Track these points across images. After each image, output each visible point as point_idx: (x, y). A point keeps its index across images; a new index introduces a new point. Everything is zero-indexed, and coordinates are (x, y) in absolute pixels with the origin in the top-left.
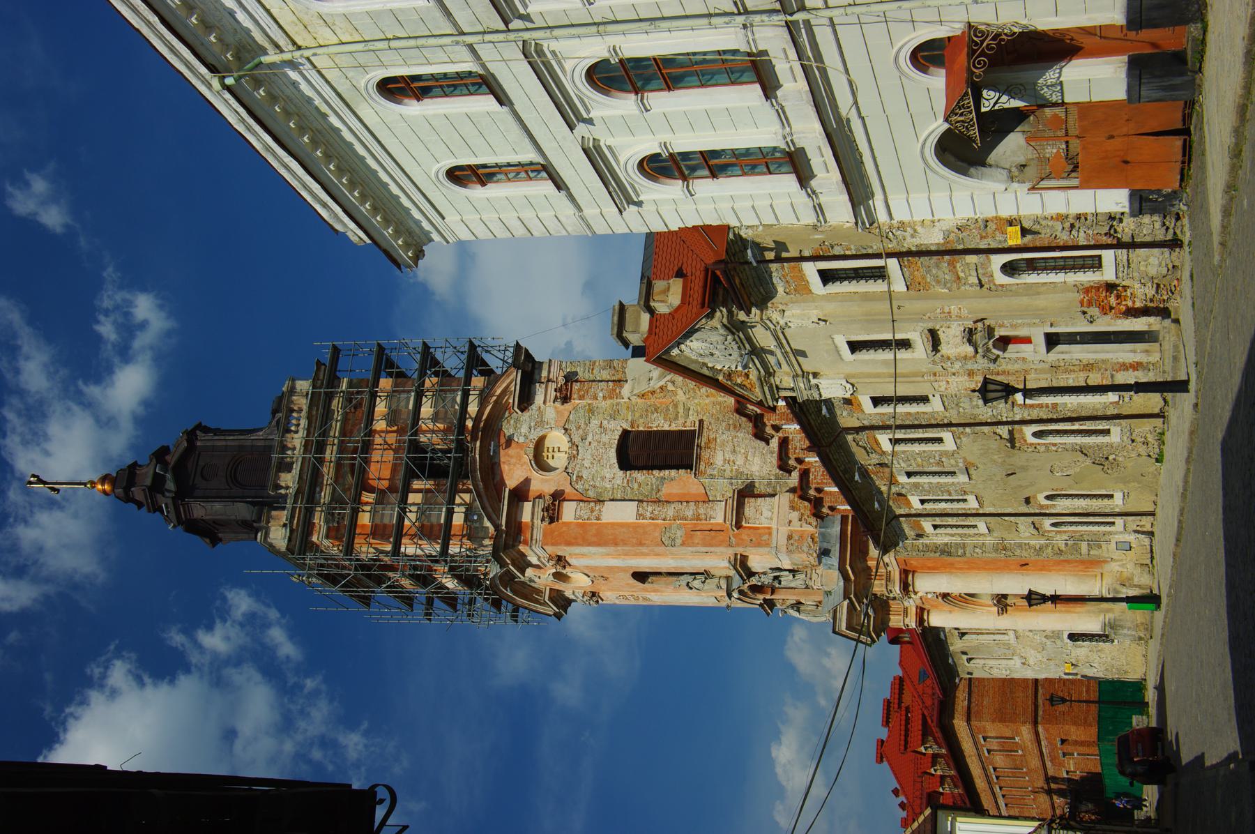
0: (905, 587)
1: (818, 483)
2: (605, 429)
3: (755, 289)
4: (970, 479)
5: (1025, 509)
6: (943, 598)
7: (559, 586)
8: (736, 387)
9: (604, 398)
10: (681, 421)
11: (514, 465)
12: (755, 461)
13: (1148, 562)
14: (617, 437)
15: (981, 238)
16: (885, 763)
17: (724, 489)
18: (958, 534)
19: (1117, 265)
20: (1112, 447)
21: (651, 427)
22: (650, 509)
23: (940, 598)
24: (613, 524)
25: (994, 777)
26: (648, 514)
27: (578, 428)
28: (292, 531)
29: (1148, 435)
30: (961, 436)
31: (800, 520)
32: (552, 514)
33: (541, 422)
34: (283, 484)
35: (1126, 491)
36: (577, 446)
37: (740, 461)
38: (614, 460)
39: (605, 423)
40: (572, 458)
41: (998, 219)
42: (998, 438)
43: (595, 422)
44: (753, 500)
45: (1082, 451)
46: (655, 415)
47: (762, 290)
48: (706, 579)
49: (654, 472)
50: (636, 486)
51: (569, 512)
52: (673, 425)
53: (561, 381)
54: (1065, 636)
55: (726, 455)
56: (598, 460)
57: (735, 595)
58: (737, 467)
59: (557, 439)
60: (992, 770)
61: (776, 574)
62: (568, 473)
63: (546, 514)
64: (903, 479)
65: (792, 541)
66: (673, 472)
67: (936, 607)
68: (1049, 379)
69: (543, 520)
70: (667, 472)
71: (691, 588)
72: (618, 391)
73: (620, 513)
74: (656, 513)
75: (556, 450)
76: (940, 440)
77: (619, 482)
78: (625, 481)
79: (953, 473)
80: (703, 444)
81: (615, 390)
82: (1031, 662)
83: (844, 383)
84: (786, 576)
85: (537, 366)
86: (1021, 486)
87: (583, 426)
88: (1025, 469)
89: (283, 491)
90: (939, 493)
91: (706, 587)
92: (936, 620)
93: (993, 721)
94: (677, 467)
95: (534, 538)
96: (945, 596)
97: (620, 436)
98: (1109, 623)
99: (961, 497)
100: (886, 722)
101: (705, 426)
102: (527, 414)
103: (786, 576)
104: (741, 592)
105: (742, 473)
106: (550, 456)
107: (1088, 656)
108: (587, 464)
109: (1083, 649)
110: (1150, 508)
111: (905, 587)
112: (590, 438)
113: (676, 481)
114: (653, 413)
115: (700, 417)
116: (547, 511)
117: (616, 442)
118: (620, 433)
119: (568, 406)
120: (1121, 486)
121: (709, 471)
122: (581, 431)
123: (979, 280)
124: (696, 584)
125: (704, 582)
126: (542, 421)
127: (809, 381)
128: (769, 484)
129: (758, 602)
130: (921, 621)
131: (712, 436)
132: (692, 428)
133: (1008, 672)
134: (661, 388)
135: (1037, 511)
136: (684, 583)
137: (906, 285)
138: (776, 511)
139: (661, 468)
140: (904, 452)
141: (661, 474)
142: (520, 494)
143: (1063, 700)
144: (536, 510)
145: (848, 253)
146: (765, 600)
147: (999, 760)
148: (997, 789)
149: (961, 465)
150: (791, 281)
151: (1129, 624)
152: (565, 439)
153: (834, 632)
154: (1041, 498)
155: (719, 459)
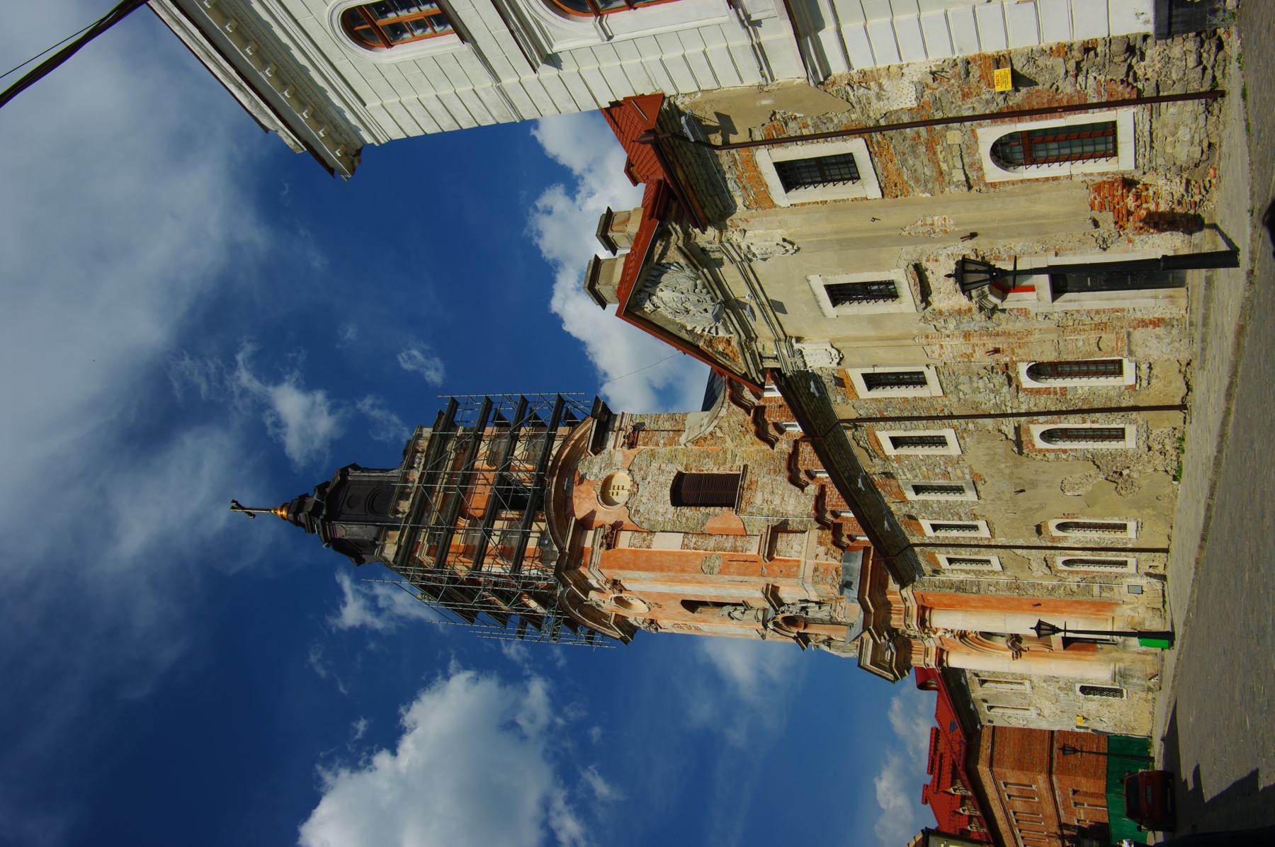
0: (922, 622)
1: (833, 506)
2: (663, 471)
3: (709, 199)
4: (979, 497)
5: (1035, 541)
6: (960, 639)
7: (623, 612)
8: (718, 356)
9: (665, 445)
10: (728, 465)
11: (584, 499)
12: (790, 502)
13: (1160, 606)
14: (672, 478)
15: (964, 95)
16: (929, 805)
17: (759, 525)
18: (973, 571)
19: (1136, 140)
20: (1127, 457)
21: (702, 471)
22: (694, 540)
23: (957, 638)
24: (661, 553)
25: (1014, 820)
27: (641, 469)
28: (399, 547)
29: (1167, 441)
30: (965, 435)
31: (826, 554)
32: (610, 541)
33: (610, 464)
34: (401, 510)
35: (1140, 520)
36: (638, 485)
37: (777, 501)
38: (668, 497)
39: (663, 466)
40: (632, 494)
41: (984, 58)
42: (1004, 437)
43: (655, 465)
45: (1094, 460)
46: (707, 460)
47: (718, 202)
48: (745, 610)
49: (701, 509)
50: (684, 520)
51: (624, 540)
52: (721, 469)
53: (630, 430)
54: (1078, 689)
57: (770, 625)
58: (773, 506)
59: (622, 479)
60: (1012, 814)
61: (805, 605)
62: (628, 507)
63: (604, 541)
64: (911, 495)
65: (818, 573)
66: (718, 509)
67: (955, 649)
68: (1056, 341)
69: (601, 546)
70: (712, 509)
71: (733, 619)
72: (676, 439)
73: (667, 543)
74: (700, 544)
75: (620, 488)
76: (941, 442)
77: (670, 516)
79: (959, 490)
80: (745, 486)
82: (1046, 713)
83: (829, 348)
84: (813, 607)
85: (612, 417)
86: (1031, 509)
87: (644, 468)
88: (1033, 484)
90: (950, 516)
91: (745, 617)
92: (955, 661)
93: (1013, 769)
94: (721, 506)
95: (593, 561)
96: (963, 636)
97: (675, 477)
98: (1119, 672)
99: (970, 523)
101: (749, 470)
102: (599, 457)
103: (813, 607)
104: (776, 624)
105: (778, 512)
106: (615, 493)
107: (1098, 711)
108: (644, 500)
109: (1094, 703)
110: (1165, 546)
111: (922, 622)
112: (649, 479)
113: (720, 517)
114: (705, 458)
115: (745, 462)
116: (606, 538)
117: (671, 482)
118: (675, 474)
119: (634, 451)
120: (1134, 512)
121: (749, 509)
122: (642, 472)
123: (966, 176)
124: (737, 614)
125: (743, 613)
126: (611, 463)
127: (792, 346)
128: (801, 522)
129: (793, 635)
130: (940, 661)
131: (754, 479)
132: (738, 472)
133: (1025, 722)
134: (711, 434)
135: (1049, 544)
136: (726, 613)
137: (880, 187)
138: (805, 545)
139: (707, 505)
140: (908, 457)
141: (707, 511)
142: (585, 524)
143: (1075, 751)
144: (597, 537)
145: (806, 132)
146: (798, 633)
147: (1018, 804)
148: (1017, 831)
149: (968, 477)
150: (748, 186)
151: (1138, 674)
152: (629, 478)
153: (859, 665)
154: (1052, 525)
155: (758, 500)
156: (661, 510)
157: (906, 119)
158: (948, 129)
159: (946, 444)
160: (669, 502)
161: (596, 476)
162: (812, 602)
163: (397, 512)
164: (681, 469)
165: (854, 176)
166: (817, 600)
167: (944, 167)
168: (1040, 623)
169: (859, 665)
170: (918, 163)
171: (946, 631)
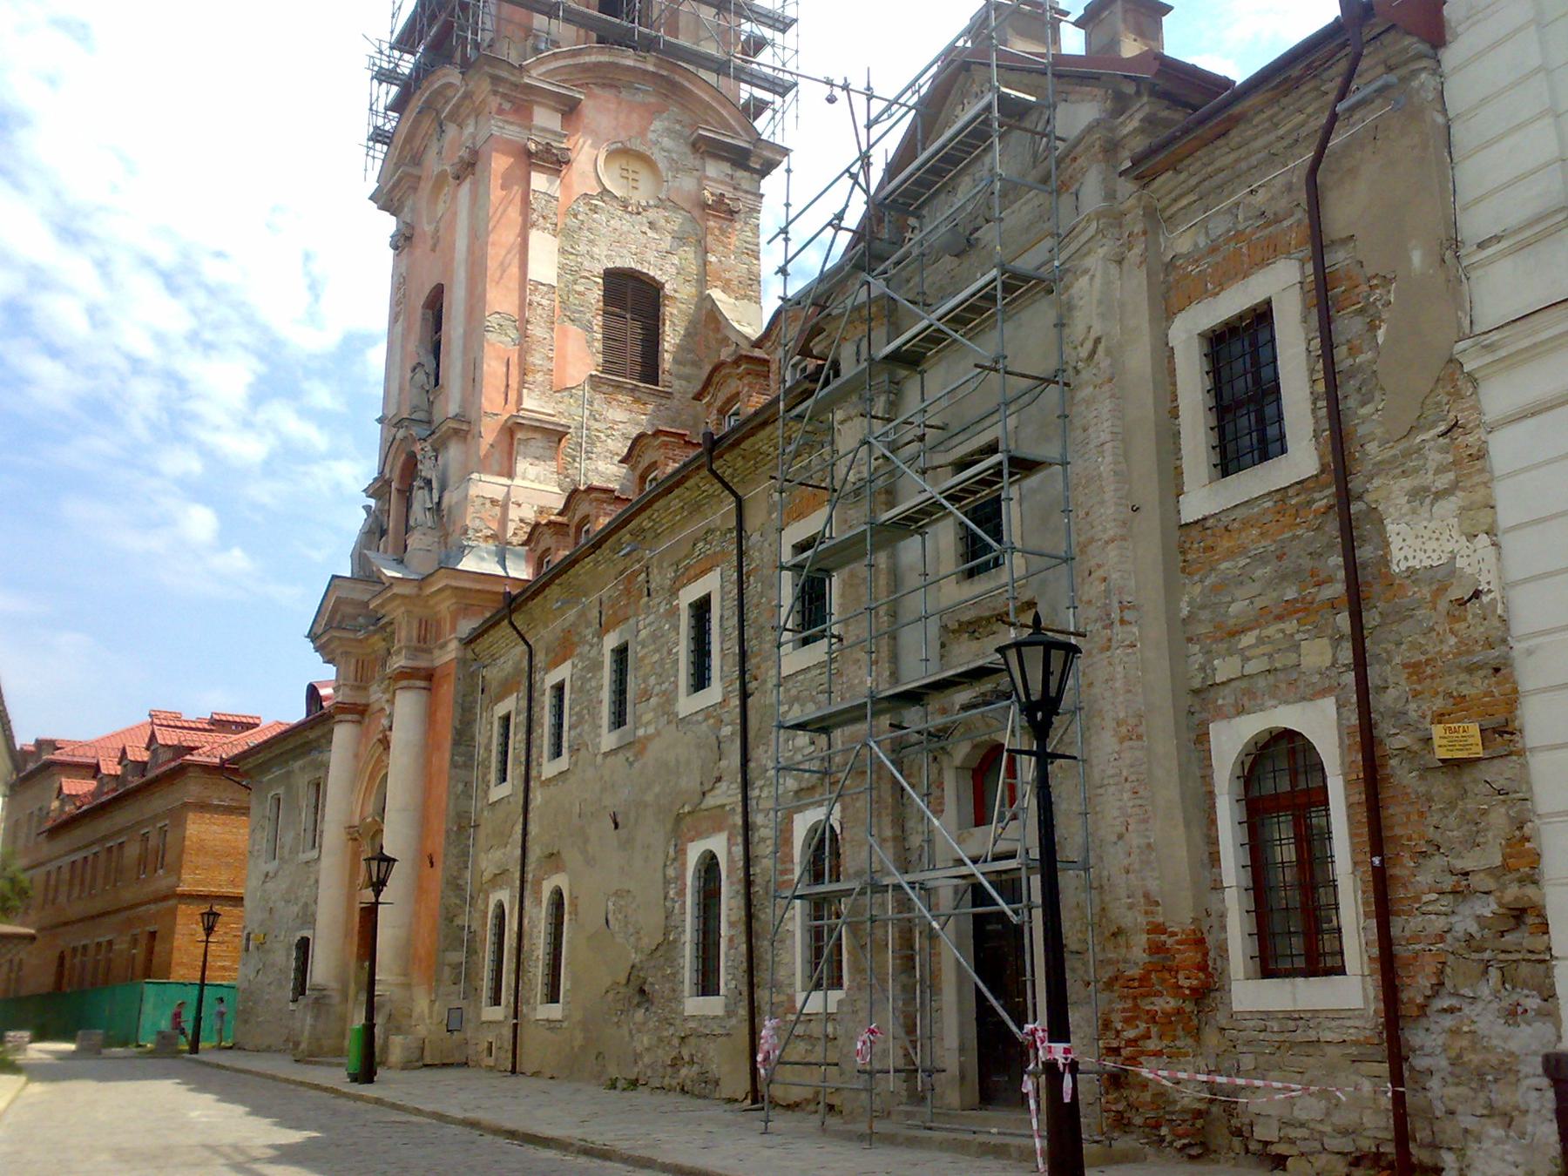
3: (1193, 181)
4: (606, 755)
5: (535, 853)
7: (426, 187)
11: (616, 118)
13: (428, 1061)
14: (652, 274)
15: (1417, 665)
18: (490, 756)
20: (670, 1000)
22: (545, 302)
23: (381, 736)
29: (696, 1068)
30: (711, 721)
31: (522, 520)
33: (676, 167)
35: (565, 1025)
36: (639, 213)
38: (619, 263)
41: (1512, 700)
42: (706, 788)
45: (666, 947)
47: (1184, 202)
54: (306, 933)
55: (621, 426)
57: (401, 434)
61: (435, 484)
64: (611, 641)
65: (488, 505)
66: (599, 345)
71: (414, 369)
74: (539, 310)
76: (700, 680)
78: (586, 274)
79: (619, 719)
81: (719, 279)
82: (270, 885)
84: (431, 498)
86: (586, 841)
88: (627, 844)
90: (577, 709)
91: (415, 391)
96: (385, 743)
97: (653, 278)
98: (324, 997)
99: (565, 744)
102: (687, 150)
105: (593, 444)
107: (273, 965)
109: (284, 958)
110: (528, 1062)
112: (650, 233)
115: (678, 396)
117: (645, 271)
119: (697, 213)
120: (578, 1016)
122: (662, 222)
124: (420, 377)
126: (677, 170)
135: (529, 877)
136: (424, 360)
137: (1205, 519)
138: (536, 485)
140: (676, 628)
141: (596, 328)
143: (209, 930)
145: (1341, 353)
146: (388, 483)
149: (641, 732)
150: (1218, 258)
154: (560, 880)
156: (595, 250)
157: (1365, 553)
158: (1336, 642)
159: (697, 690)
160: (611, 265)
161: (656, 143)
162: (440, 498)
165: (1228, 463)
166: (445, 504)
167: (1248, 639)
168: (390, 861)
169: (334, 577)
170: (1254, 588)
171: (391, 716)
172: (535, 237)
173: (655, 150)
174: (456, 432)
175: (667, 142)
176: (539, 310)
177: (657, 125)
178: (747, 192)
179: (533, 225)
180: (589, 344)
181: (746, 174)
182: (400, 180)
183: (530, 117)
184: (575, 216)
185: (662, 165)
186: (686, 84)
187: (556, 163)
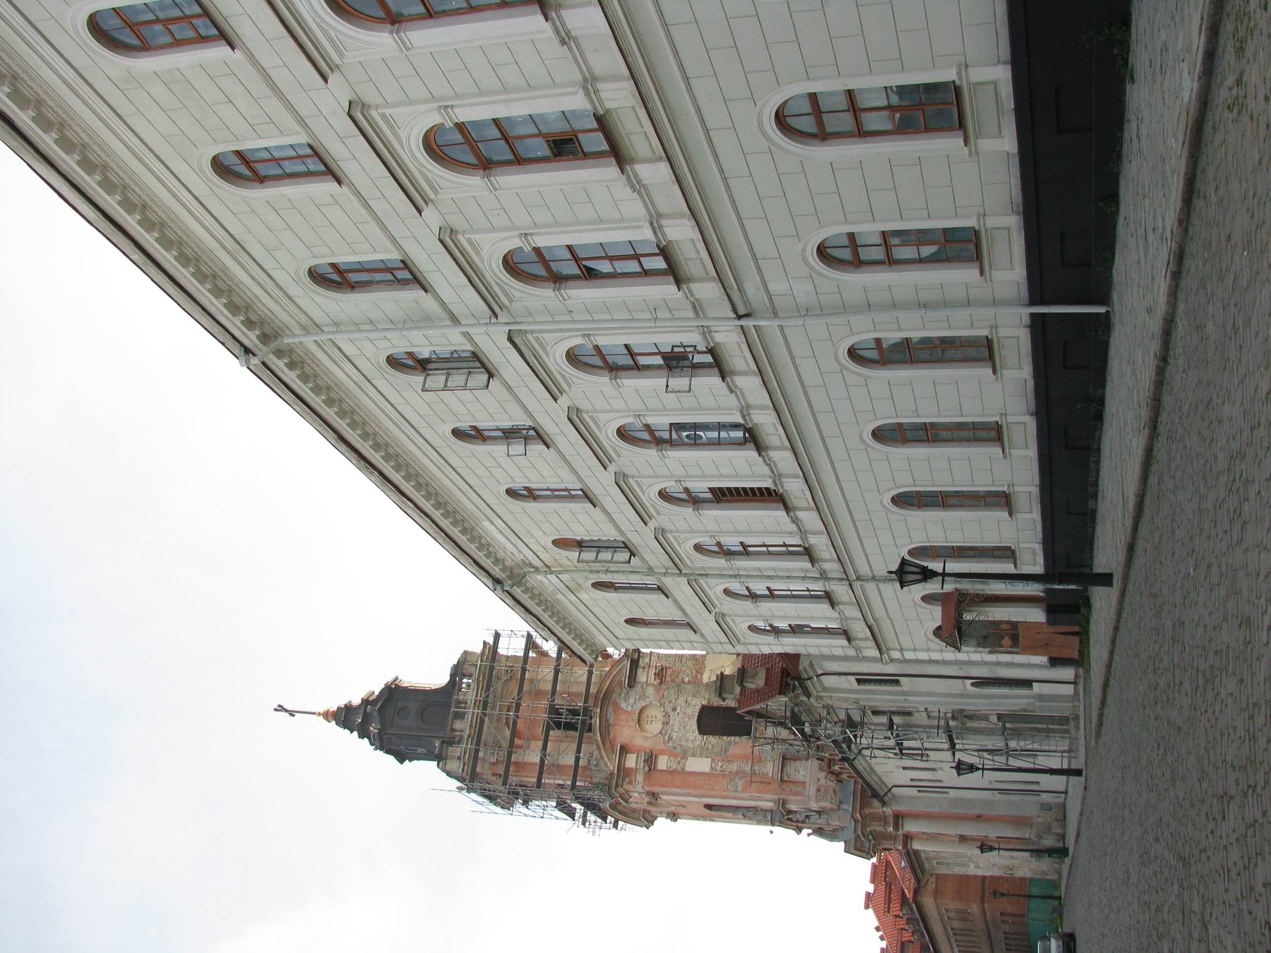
14: (698, 711)
16: (870, 910)
22: (720, 764)
26: (718, 768)
33: (643, 697)
40: (666, 723)
43: (681, 700)
44: (793, 762)
49: (724, 737)
51: (663, 763)
56: (683, 726)
66: (737, 739)
70: (733, 738)
73: (699, 765)
74: (724, 767)
81: (697, 677)
89: (458, 733)
93: (953, 899)
94: (740, 735)
100: (873, 880)
102: (634, 690)
108: (676, 728)
112: (678, 710)
116: (647, 761)
119: (664, 687)
143: (1003, 894)
156: (690, 738)
163: (453, 730)
164: (705, 703)
172: (688, 769)
173: (636, 707)
174: (783, 805)
175: (631, 701)
176: (724, 767)
177: (623, 706)
178: (650, 660)
179: (683, 769)
180: (735, 743)
181: (641, 660)
182: (645, 819)
183: (631, 769)
184: (675, 748)
185: (643, 704)
186: (604, 691)
187: (651, 759)
